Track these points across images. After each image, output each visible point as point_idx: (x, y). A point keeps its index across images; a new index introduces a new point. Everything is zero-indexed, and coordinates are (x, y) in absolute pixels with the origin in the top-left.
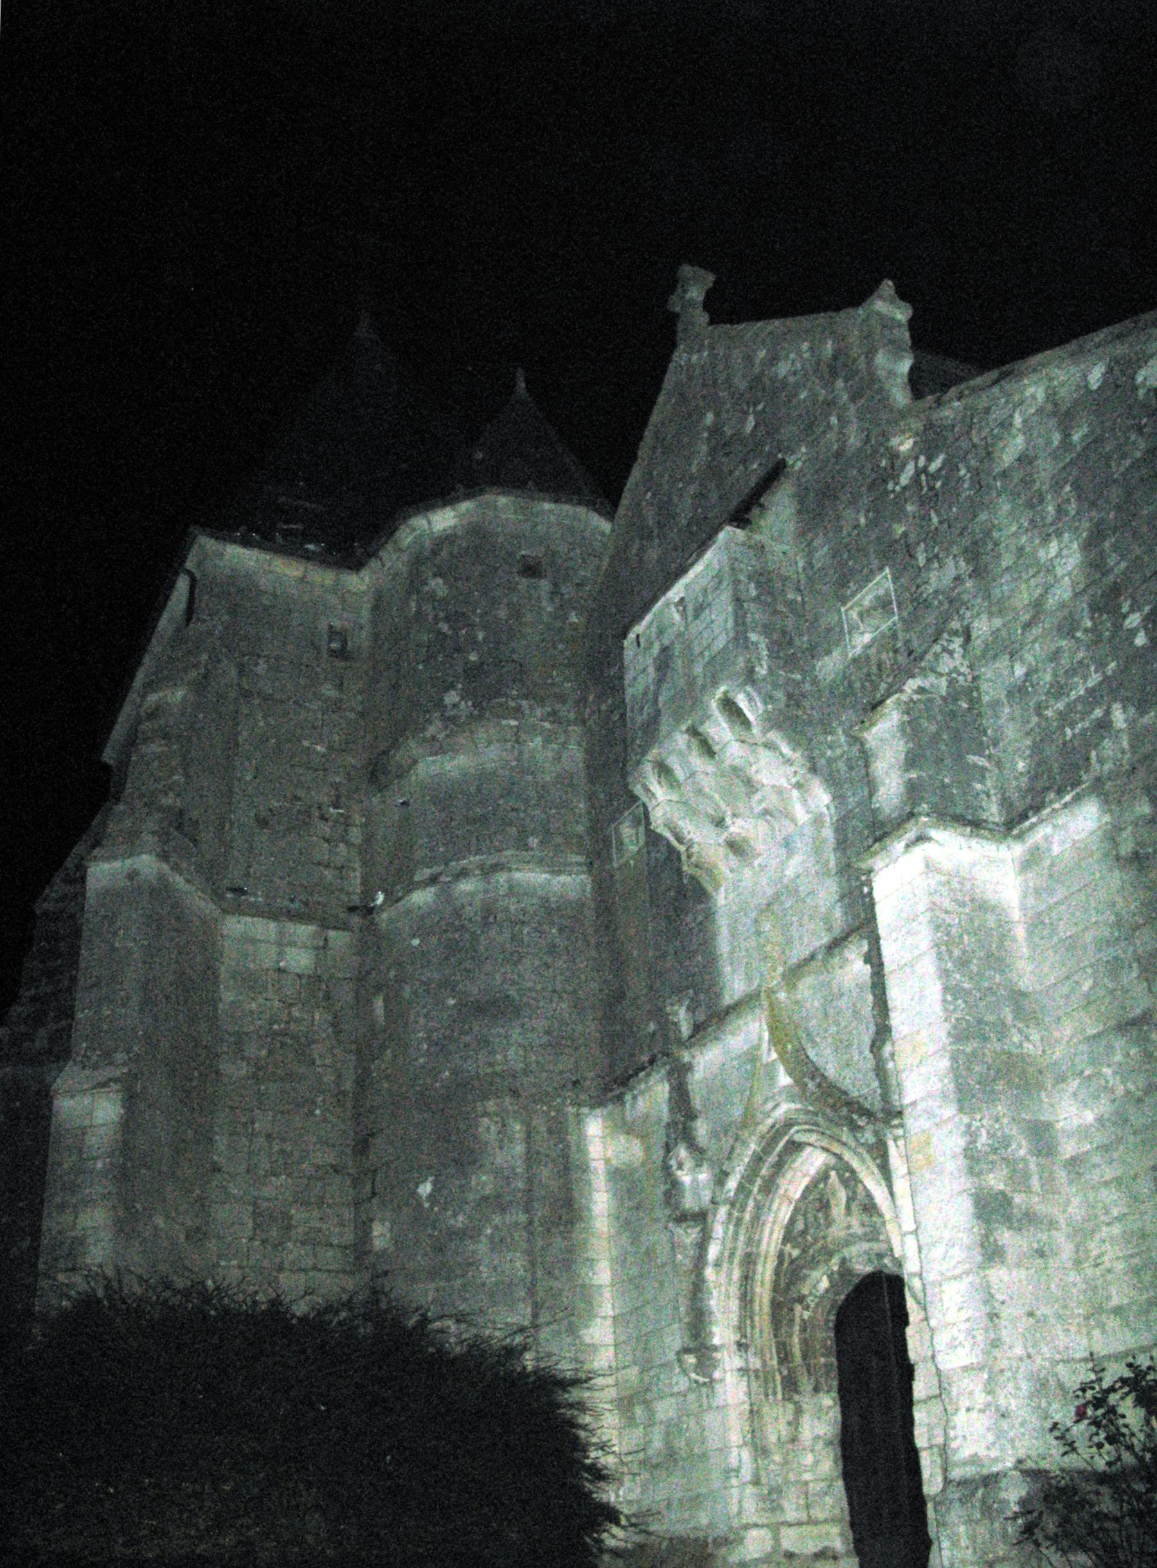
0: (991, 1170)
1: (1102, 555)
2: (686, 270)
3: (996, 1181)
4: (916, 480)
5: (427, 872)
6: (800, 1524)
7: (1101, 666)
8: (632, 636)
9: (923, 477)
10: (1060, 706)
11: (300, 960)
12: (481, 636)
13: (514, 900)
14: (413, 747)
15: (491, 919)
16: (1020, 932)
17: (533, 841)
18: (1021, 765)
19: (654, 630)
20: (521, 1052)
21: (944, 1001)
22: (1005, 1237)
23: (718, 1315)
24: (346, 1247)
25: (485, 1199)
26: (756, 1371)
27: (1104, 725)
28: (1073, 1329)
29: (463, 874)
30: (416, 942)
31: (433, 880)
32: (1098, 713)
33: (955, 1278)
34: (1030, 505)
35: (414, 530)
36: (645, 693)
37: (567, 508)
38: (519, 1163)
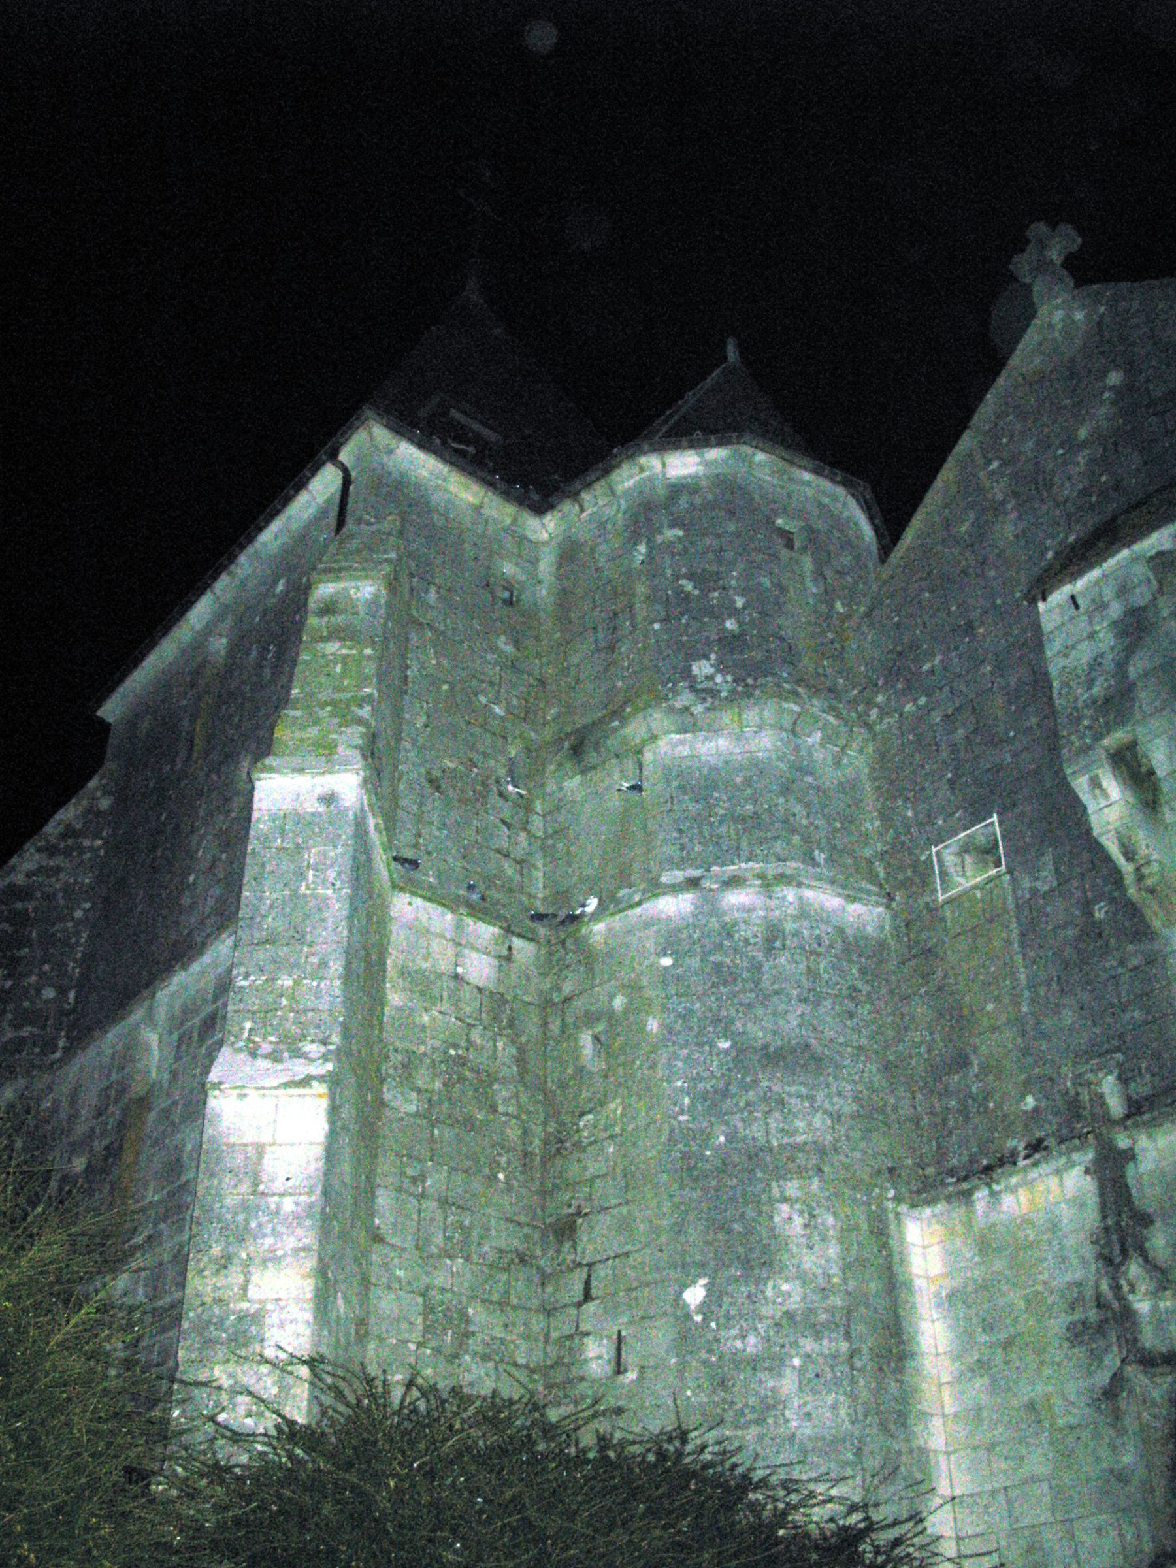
2: (1040, 228)
5: (679, 875)
11: (479, 969)
12: (740, 602)
13: (806, 923)
14: (658, 719)
15: (778, 944)
17: (821, 857)
20: (829, 1122)
24: (533, 1371)
25: (789, 1315)
29: (734, 882)
30: (667, 962)
31: (693, 883)
35: (642, 469)
37: (825, 484)
38: (835, 1270)
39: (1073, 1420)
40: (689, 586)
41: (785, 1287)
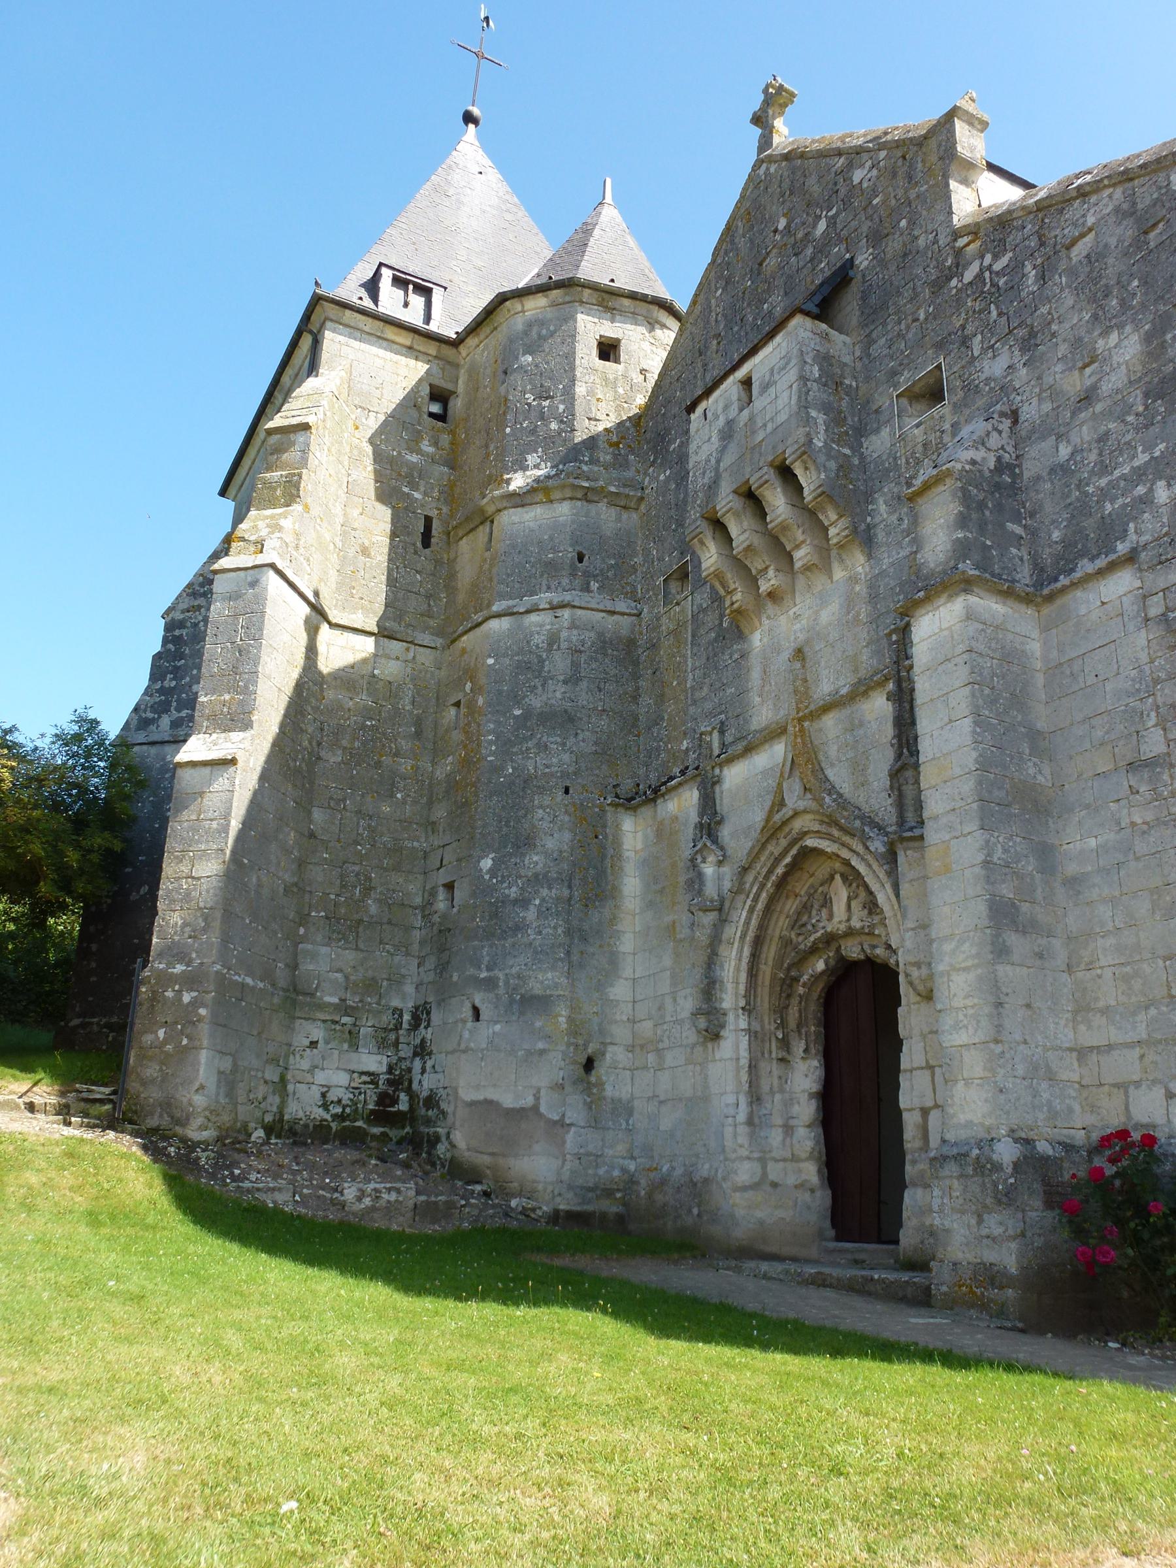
0: (1004, 881)
1: (1163, 346)
3: (1007, 891)
4: (979, 276)
6: (784, 1160)
7: (1148, 448)
8: (699, 410)
9: (987, 274)
10: (1103, 482)
16: (1040, 679)
17: (594, 586)
18: (1056, 535)
19: (721, 405)
21: (974, 732)
22: (1012, 939)
23: (730, 987)
26: (756, 1032)
27: (1147, 501)
28: (1063, 1022)
30: (491, 661)
32: (1141, 490)
33: (965, 969)
34: (1093, 299)
36: (708, 461)
40: (530, 397)
41: (535, 858)
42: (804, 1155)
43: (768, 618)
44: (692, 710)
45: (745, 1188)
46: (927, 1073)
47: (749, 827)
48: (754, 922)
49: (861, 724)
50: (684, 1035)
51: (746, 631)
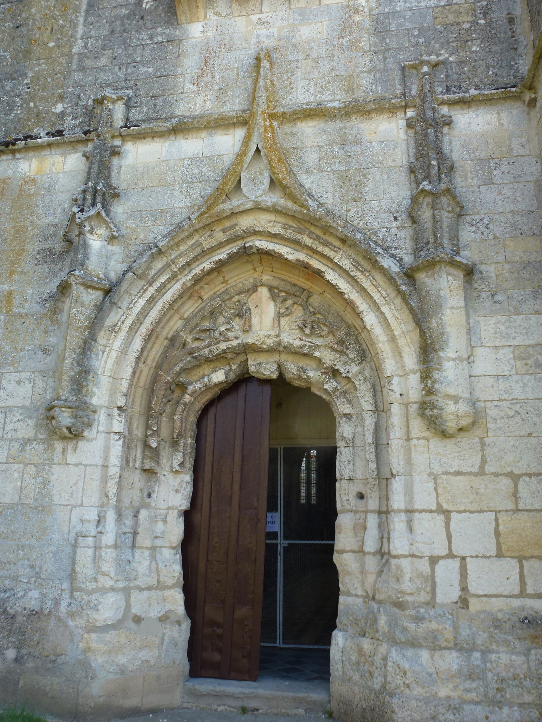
6: (149, 588)
39: (23, 311)
42: (170, 582)
43: (217, 14)
44: (77, 76)
45: (106, 628)
46: (440, 519)
47: (162, 211)
48: (155, 313)
49: (357, 141)
50: (9, 426)
51: (182, 18)
